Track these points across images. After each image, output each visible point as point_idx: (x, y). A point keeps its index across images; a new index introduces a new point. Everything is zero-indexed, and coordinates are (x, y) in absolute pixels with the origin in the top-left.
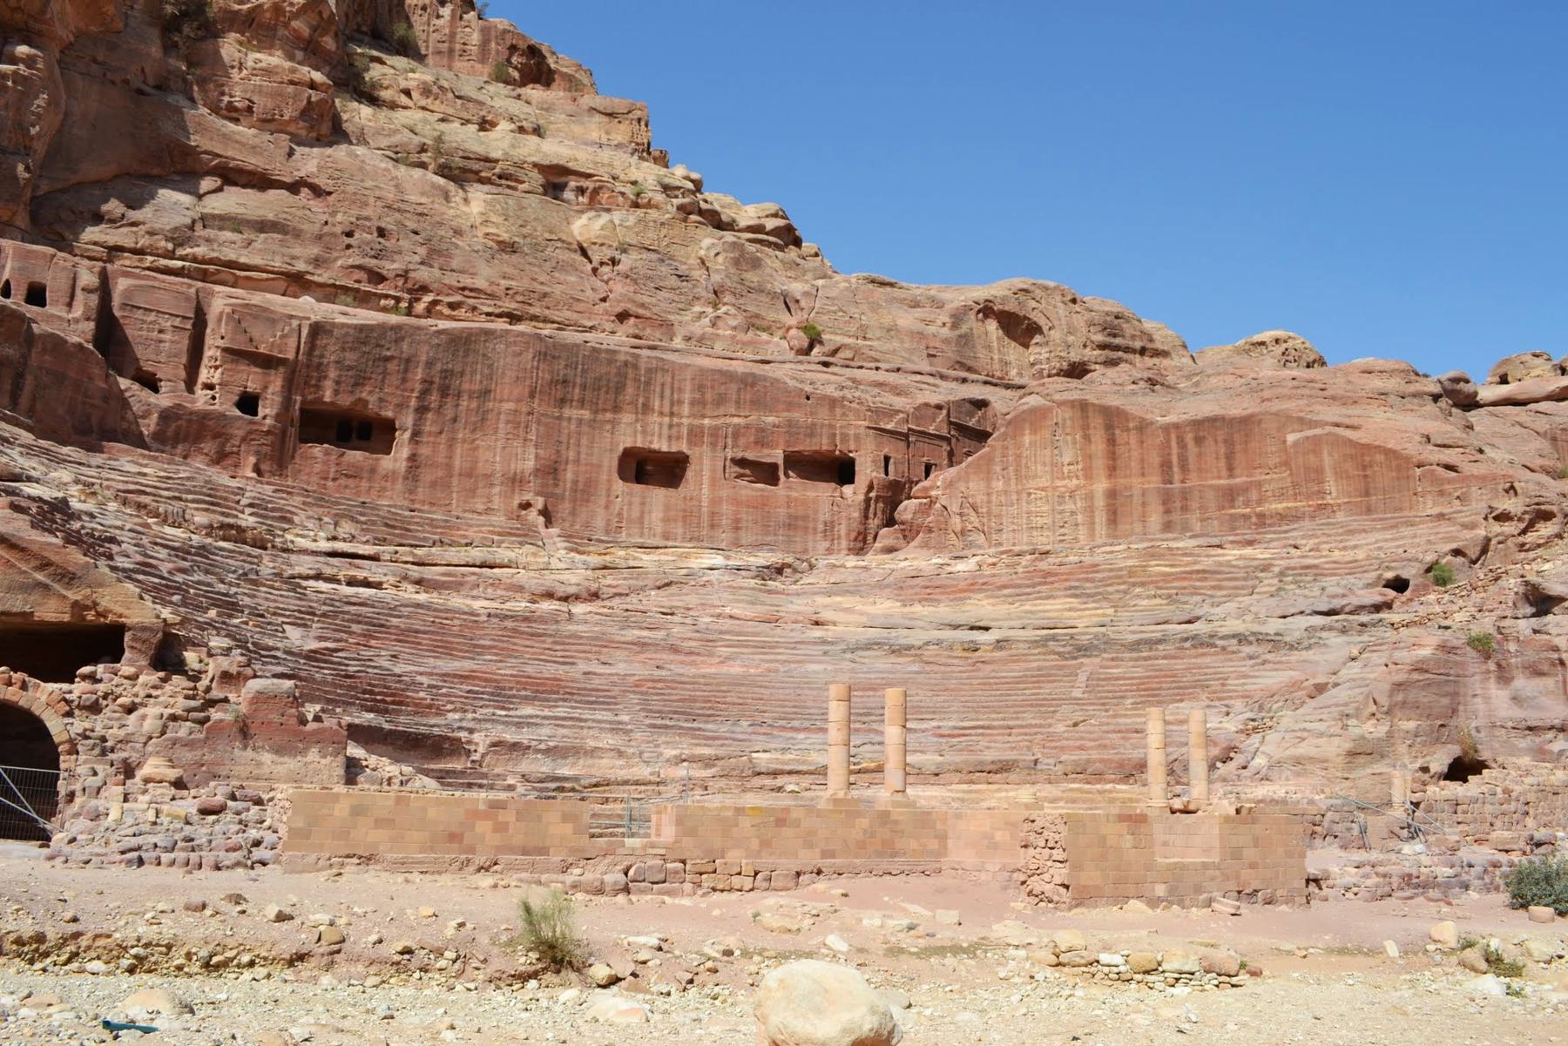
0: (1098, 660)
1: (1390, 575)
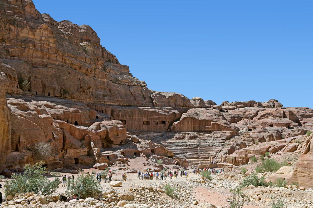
1: (223, 139)
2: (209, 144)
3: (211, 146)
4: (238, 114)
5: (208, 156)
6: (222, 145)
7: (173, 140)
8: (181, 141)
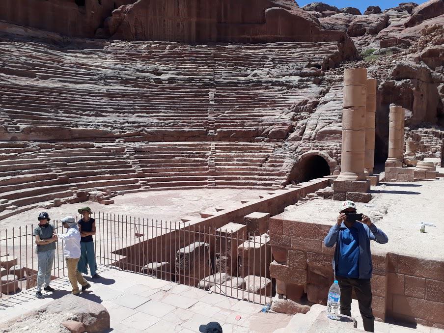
0: (214, 90)
2: (254, 79)
3: (267, 88)
4: (333, 23)
5: (253, 128)
6: (319, 83)
7: (104, 62)
8: (139, 66)
